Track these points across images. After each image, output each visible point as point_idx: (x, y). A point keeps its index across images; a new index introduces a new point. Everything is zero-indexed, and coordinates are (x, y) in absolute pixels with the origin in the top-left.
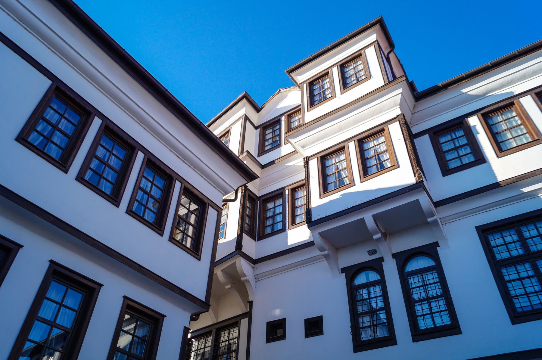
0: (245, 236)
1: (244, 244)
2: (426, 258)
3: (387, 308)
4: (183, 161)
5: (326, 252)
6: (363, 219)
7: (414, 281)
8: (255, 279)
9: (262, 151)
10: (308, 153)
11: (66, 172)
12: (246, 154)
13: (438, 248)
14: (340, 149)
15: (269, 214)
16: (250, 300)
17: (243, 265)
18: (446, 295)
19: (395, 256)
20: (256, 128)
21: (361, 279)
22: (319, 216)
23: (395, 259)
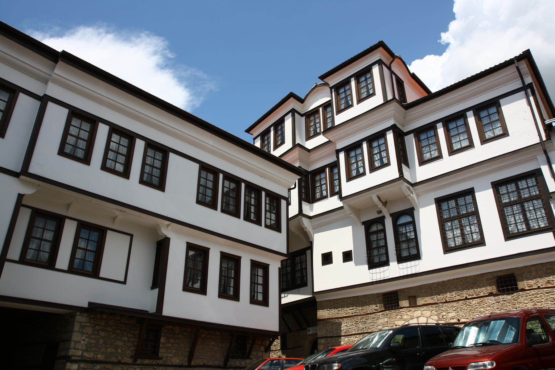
0: (303, 202)
1: (303, 209)
2: (408, 216)
3: (386, 246)
6: (371, 197)
9: (308, 138)
10: (339, 147)
14: (357, 145)
16: (311, 241)
17: (305, 221)
19: (391, 215)
20: (302, 115)
21: (374, 228)
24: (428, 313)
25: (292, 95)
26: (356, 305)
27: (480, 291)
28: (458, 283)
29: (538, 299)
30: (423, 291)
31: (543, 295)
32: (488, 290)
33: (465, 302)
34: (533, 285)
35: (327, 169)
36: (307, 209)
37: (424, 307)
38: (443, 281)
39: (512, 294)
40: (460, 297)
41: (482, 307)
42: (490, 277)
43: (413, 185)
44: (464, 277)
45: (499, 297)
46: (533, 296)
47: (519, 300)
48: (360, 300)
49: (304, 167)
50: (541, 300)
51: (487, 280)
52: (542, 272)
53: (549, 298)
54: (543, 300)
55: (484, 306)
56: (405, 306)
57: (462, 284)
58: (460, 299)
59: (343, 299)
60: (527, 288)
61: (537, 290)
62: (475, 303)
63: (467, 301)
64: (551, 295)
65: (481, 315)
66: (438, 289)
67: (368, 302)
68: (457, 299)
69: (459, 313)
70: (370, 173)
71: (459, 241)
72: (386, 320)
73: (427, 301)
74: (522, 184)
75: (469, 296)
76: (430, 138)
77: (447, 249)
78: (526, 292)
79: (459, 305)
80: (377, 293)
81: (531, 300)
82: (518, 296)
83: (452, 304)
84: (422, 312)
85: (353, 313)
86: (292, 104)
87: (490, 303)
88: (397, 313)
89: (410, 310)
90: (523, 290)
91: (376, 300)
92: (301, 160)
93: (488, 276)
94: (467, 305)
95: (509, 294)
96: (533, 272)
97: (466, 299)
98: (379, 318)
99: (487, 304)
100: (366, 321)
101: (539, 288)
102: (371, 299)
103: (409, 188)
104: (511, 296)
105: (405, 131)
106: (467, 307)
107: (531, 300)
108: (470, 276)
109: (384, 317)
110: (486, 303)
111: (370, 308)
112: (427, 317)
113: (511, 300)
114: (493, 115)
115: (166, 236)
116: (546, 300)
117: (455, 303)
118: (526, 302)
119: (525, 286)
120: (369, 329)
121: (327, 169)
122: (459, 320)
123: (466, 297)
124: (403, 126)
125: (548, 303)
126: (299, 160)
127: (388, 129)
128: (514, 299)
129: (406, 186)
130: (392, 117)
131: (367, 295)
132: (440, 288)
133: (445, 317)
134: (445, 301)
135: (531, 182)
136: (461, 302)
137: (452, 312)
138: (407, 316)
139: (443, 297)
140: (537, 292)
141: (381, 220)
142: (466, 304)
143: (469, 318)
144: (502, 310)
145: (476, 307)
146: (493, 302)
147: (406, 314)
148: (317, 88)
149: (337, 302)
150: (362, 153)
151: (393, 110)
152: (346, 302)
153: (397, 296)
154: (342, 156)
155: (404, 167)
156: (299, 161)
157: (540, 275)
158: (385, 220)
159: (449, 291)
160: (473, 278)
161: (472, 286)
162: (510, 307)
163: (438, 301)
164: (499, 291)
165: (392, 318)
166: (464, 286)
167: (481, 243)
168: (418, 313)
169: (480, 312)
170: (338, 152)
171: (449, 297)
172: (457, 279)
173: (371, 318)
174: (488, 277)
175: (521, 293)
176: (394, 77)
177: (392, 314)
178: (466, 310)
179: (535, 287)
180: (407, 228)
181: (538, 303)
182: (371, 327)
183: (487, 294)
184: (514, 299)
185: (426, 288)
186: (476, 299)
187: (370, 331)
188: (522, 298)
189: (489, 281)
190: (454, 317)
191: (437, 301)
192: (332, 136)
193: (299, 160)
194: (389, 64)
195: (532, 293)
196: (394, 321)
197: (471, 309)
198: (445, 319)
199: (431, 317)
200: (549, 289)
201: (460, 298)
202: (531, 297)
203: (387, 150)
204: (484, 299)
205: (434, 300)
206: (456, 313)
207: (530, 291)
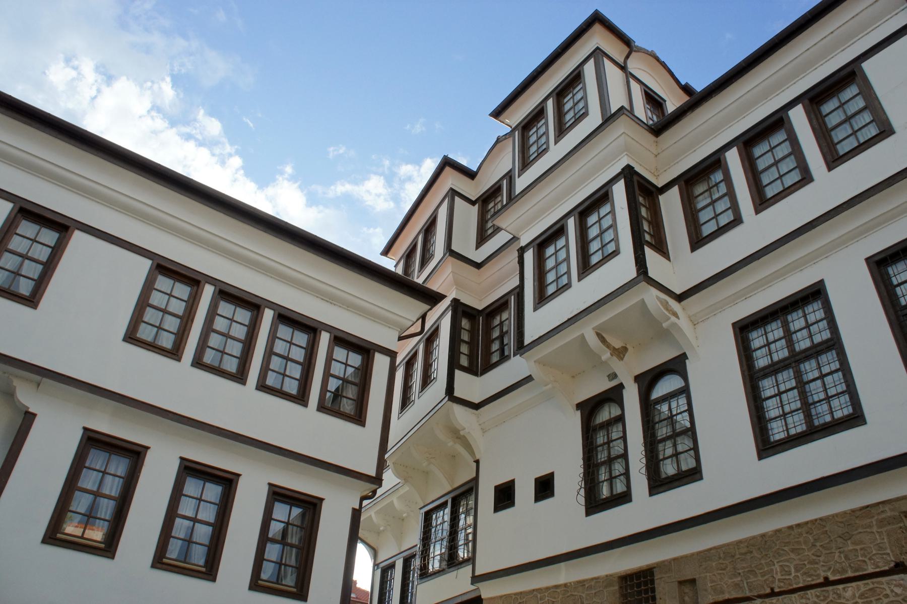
0: (458, 373)
3: (625, 456)
4: (331, 303)
5: (550, 386)
6: (583, 336)
8: (482, 429)
10: (523, 242)
11: (179, 360)
14: (557, 232)
15: (496, 334)
16: (477, 459)
19: (637, 379)
20: (473, 203)
22: (532, 337)
27: (864, 559)
28: (801, 539)
30: (714, 564)
33: (824, 593)
35: (513, 297)
36: (467, 385)
38: (763, 536)
42: (889, 514)
43: (680, 298)
44: (816, 520)
48: (569, 594)
49: (466, 300)
51: (881, 523)
57: (812, 541)
58: (809, 583)
59: (535, 593)
62: (854, 595)
63: (830, 588)
66: (752, 557)
67: (587, 599)
68: (801, 585)
70: (579, 280)
71: (797, 424)
73: (723, 592)
75: (834, 573)
76: (715, 188)
87: (896, 594)
94: (829, 600)
97: (827, 582)
102: (593, 592)
103: (667, 303)
105: (660, 186)
108: (833, 516)
114: (851, 102)
115: (28, 408)
117: (796, 595)
121: (513, 297)
123: (826, 578)
124: (657, 177)
126: (455, 287)
129: (657, 296)
130: (622, 153)
132: (755, 554)
134: (768, 591)
136: (813, 591)
139: (765, 581)
142: (826, 598)
148: (499, 145)
149: (521, 601)
150: (567, 246)
151: (623, 135)
152: (541, 599)
153: (652, 582)
154: (529, 256)
155: (648, 252)
156: (456, 288)
158: (625, 392)
159: (778, 562)
160: (840, 522)
161: (841, 546)
163: (751, 590)
166: (818, 544)
170: (522, 251)
171: (779, 580)
172: (798, 525)
174: (883, 516)
176: (636, 88)
180: (674, 404)
183: (887, 568)
185: (720, 558)
186: (854, 584)
189: (885, 529)
191: (747, 592)
194: (623, 62)
201: (809, 581)
203: (614, 226)
205: (741, 588)
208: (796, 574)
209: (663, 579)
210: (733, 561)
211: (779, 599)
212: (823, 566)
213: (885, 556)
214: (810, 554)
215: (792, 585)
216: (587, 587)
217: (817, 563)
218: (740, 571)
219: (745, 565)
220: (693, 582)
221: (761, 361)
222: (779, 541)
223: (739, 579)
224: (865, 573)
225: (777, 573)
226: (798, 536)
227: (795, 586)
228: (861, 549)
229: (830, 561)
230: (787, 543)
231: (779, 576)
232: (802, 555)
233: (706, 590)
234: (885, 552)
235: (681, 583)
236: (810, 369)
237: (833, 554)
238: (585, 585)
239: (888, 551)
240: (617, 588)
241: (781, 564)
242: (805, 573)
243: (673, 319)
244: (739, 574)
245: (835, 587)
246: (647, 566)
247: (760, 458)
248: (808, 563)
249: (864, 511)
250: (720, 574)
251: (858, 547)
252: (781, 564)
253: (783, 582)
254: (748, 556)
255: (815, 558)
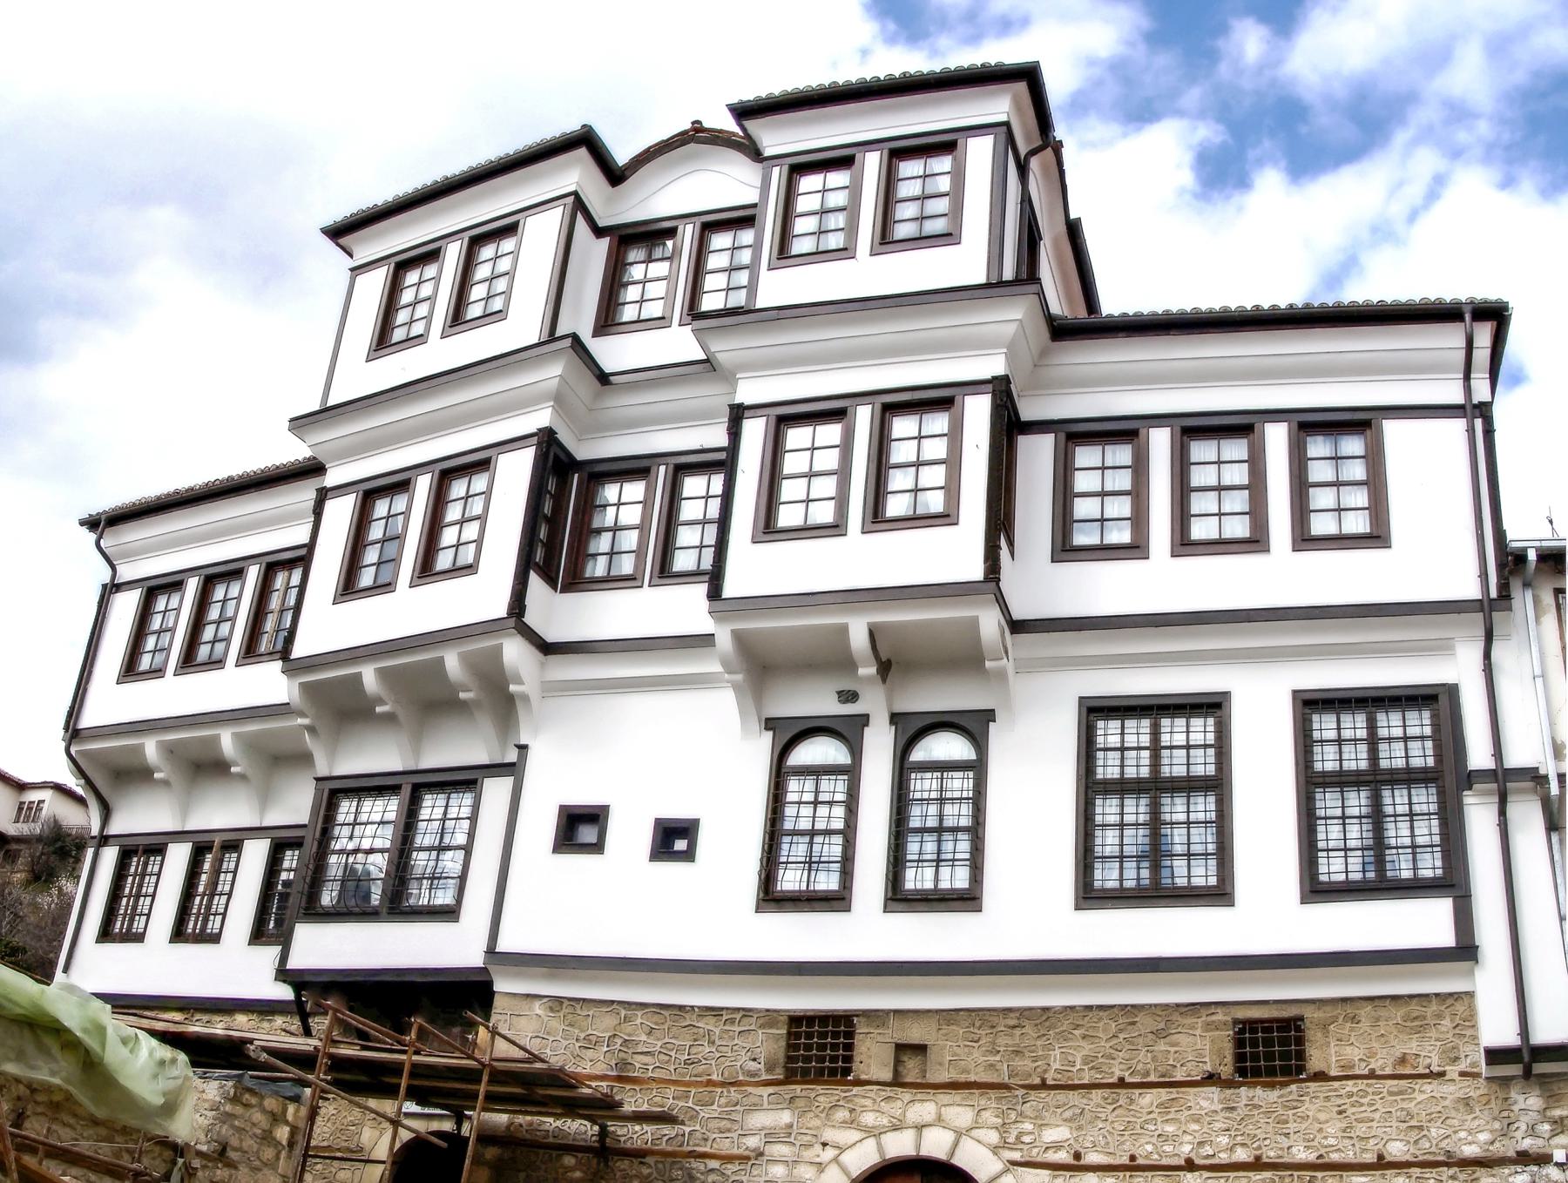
3: (849, 834)
7: (922, 785)
12: (568, 342)
13: (991, 723)
17: (515, 651)
18: (976, 831)
19: (895, 718)
23: (894, 727)
24: (960, 1115)
25: (586, 140)
26: (667, 1040)
29: (1363, 1109)
31: (1381, 1099)
32: (1205, 1062)
33: (1115, 1095)
34: (1354, 1065)
37: (954, 1092)
38: (1045, 1009)
39: (1284, 1085)
40: (1100, 1077)
41: (1172, 1119)
43: (1018, 627)
44: (1126, 1006)
45: (1237, 1091)
46: (1347, 1101)
47: (1304, 1108)
49: (565, 437)
50: (1370, 1115)
52: (1390, 1023)
53: (1396, 1111)
54: (1377, 1116)
55: (1179, 1117)
56: (874, 1078)
58: (1097, 1081)
59: (615, 1006)
60: (1333, 1073)
61: (1365, 1081)
63: (1125, 1091)
64: (1402, 1099)
65: (1162, 1146)
68: (1087, 1082)
69: (1084, 1133)
71: (1134, 875)
72: (786, 1117)
74: (1390, 723)
77: (1089, 895)
78: (1330, 1083)
79: (1090, 1102)
80: (768, 1010)
81: (1340, 1113)
82: (1302, 1096)
83: (1061, 1096)
84: (943, 1109)
85: (651, 1068)
86: (574, 174)
88: (837, 1098)
89: (892, 1095)
90: (1320, 1076)
91: (760, 1032)
92: (559, 401)
93: (1213, 1013)
95: (1272, 1086)
96: (1363, 1020)
98: (755, 1105)
99: (1190, 1112)
100: (697, 1108)
101: (1372, 1075)
104: (1277, 1093)
106: (1116, 1112)
107: (1340, 1113)
109: (779, 1106)
110: (1190, 1108)
111: (728, 1064)
112: (955, 1131)
113: (1275, 1105)
116: (1387, 1116)
117: (1076, 1093)
118: (1322, 1116)
119: (1329, 1066)
120: (706, 1140)
122: (1077, 1156)
123: (1122, 1080)
125: (1391, 1127)
127: (974, 386)
128: (1287, 1104)
131: (722, 1009)
133: (1027, 1139)
134: (1037, 1081)
135: (1419, 722)
136: (1100, 1091)
137: (1058, 1126)
138: (878, 1114)
140: (1363, 1087)
141: (849, 731)
143: (1119, 1153)
144: (1239, 1138)
145: (1151, 1116)
146: (1213, 1108)
147: (876, 1108)
153: (850, 1035)
154: (754, 432)
156: (553, 406)
157: (1383, 1032)
159: (1060, 1048)
162: (1270, 1129)
164: (1242, 1072)
165: (812, 1114)
166: (1122, 1036)
167: (1220, 894)
168: (924, 1109)
169: (1159, 1135)
170: (738, 414)
172: (1101, 1008)
173: (723, 1100)
174: (1214, 1018)
175: (1313, 1086)
177: (818, 1098)
178: (1113, 1122)
179: (1357, 1072)
181: (1361, 1125)
182: (715, 1136)
183: (1199, 1078)
184: (1287, 1104)
187: (707, 1149)
188: (1311, 1102)
190: (1065, 1141)
192: (727, 348)
193: (555, 402)
195: (1348, 1089)
196: (818, 1128)
197: (1129, 1122)
198: (1026, 1147)
199: (975, 1133)
200: (1401, 1081)
201: (1098, 1077)
202: (1343, 1102)
204: (1183, 1093)
205: (997, 1070)
206: (1071, 1128)
207: (1344, 1082)
208: (1083, 1067)
209: (872, 1035)
210: (992, 1033)
211: (1050, 1094)
212: (1121, 1063)
213: (1201, 1064)
214: (1108, 1045)
215: (1073, 1080)
216: (726, 1020)
217: (1114, 1059)
218: (1002, 1049)
219: (1010, 1042)
220: (920, 1049)
221: (1108, 768)
222: (1068, 1022)
223: (998, 1058)
224: (1174, 1079)
225: (1055, 1061)
226: (1095, 1020)
227: (1076, 1082)
228: (1176, 1052)
229: (1132, 1059)
230: (1078, 1026)
231: (1057, 1066)
232: (1098, 1045)
233: (940, 1064)
234: (1203, 1060)
235: (902, 1049)
236: (1175, 808)
237: (1136, 1052)
238: (722, 1015)
239: (1207, 1059)
240: (785, 1032)
241: (1063, 1050)
242: (1092, 1068)
243: (1005, 659)
244: (999, 1051)
245: (1130, 1091)
246: (845, 1011)
247: (1077, 908)
248: (1102, 1056)
249: (1193, 1007)
250: (966, 1046)
251: (1173, 1049)
252: (1063, 1050)
253: (1060, 1073)
254: (1018, 1032)
255: (1113, 1051)
